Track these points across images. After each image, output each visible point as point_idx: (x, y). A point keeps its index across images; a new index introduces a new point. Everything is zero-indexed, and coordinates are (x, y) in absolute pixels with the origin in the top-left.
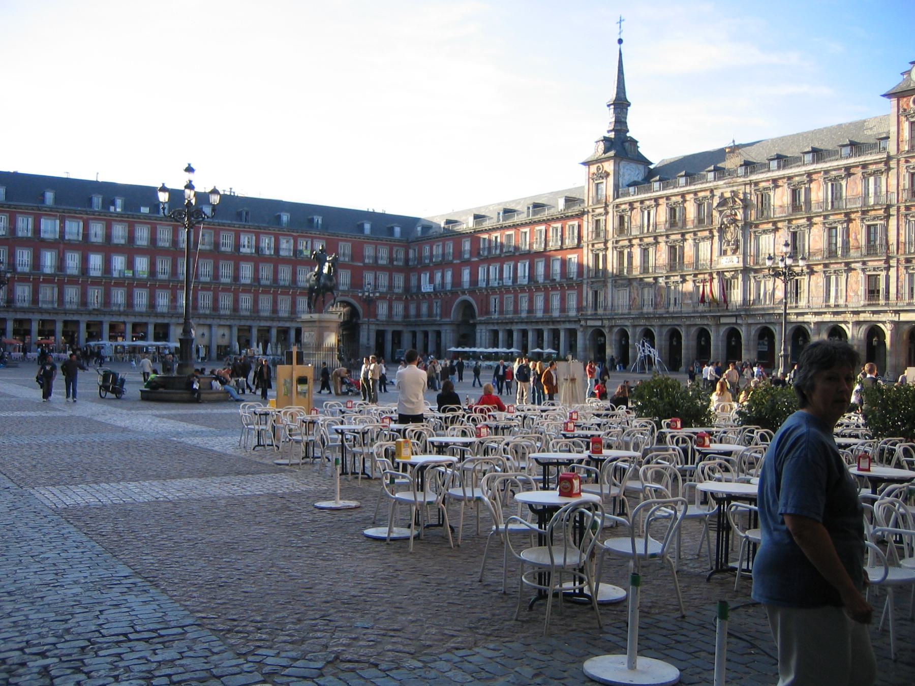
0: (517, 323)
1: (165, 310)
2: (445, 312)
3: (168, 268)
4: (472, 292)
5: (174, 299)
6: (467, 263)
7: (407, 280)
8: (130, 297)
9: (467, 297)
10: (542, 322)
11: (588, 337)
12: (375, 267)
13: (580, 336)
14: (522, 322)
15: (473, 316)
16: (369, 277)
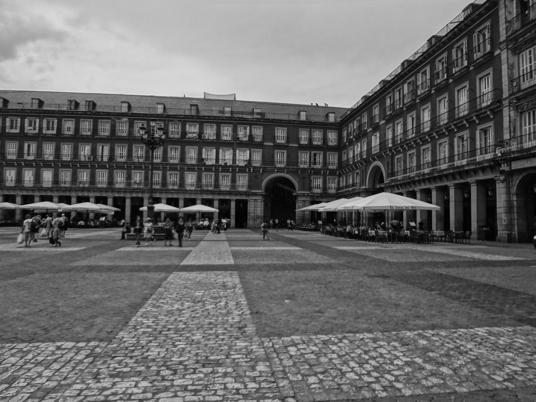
0: (419, 182)
1: (122, 186)
2: (363, 182)
3: (125, 153)
4: (380, 157)
5: (129, 177)
6: (376, 128)
7: (340, 158)
8: (93, 177)
9: (378, 163)
10: (447, 176)
11: (514, 190)
12: (310, 147)
13: (501, 189)
14: (424, 181)
15: (381, 181)
16: (304, 158)
